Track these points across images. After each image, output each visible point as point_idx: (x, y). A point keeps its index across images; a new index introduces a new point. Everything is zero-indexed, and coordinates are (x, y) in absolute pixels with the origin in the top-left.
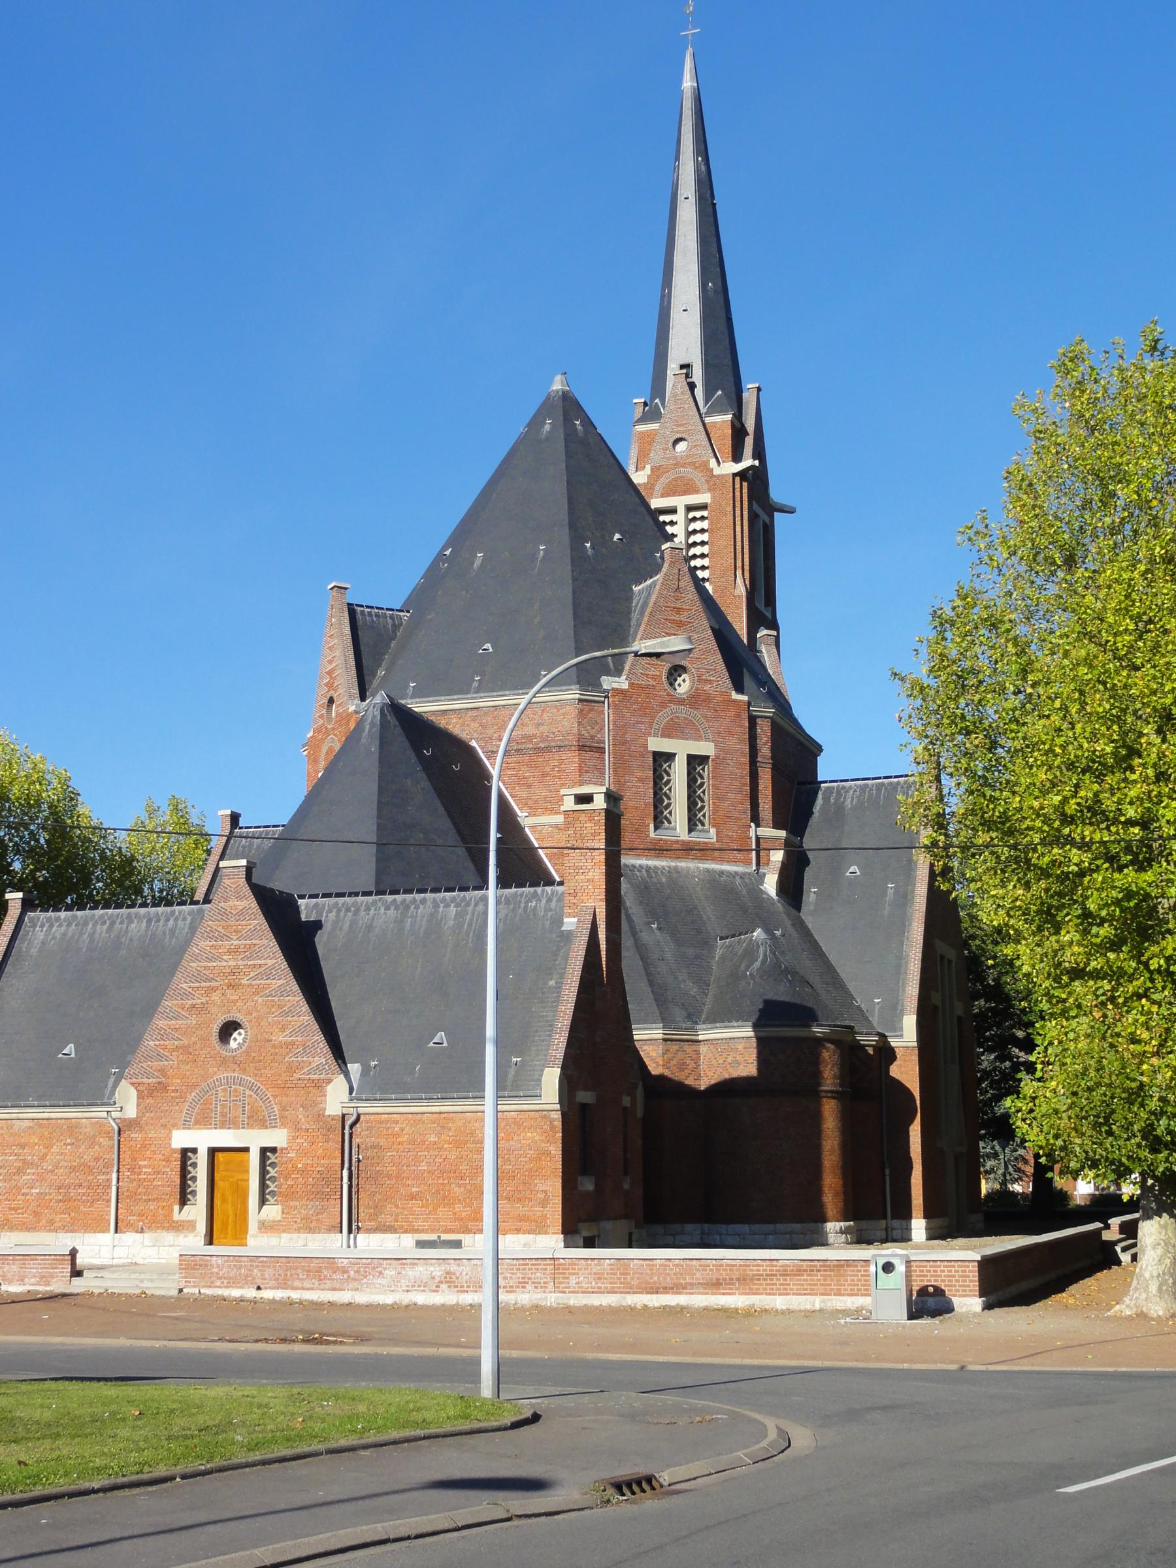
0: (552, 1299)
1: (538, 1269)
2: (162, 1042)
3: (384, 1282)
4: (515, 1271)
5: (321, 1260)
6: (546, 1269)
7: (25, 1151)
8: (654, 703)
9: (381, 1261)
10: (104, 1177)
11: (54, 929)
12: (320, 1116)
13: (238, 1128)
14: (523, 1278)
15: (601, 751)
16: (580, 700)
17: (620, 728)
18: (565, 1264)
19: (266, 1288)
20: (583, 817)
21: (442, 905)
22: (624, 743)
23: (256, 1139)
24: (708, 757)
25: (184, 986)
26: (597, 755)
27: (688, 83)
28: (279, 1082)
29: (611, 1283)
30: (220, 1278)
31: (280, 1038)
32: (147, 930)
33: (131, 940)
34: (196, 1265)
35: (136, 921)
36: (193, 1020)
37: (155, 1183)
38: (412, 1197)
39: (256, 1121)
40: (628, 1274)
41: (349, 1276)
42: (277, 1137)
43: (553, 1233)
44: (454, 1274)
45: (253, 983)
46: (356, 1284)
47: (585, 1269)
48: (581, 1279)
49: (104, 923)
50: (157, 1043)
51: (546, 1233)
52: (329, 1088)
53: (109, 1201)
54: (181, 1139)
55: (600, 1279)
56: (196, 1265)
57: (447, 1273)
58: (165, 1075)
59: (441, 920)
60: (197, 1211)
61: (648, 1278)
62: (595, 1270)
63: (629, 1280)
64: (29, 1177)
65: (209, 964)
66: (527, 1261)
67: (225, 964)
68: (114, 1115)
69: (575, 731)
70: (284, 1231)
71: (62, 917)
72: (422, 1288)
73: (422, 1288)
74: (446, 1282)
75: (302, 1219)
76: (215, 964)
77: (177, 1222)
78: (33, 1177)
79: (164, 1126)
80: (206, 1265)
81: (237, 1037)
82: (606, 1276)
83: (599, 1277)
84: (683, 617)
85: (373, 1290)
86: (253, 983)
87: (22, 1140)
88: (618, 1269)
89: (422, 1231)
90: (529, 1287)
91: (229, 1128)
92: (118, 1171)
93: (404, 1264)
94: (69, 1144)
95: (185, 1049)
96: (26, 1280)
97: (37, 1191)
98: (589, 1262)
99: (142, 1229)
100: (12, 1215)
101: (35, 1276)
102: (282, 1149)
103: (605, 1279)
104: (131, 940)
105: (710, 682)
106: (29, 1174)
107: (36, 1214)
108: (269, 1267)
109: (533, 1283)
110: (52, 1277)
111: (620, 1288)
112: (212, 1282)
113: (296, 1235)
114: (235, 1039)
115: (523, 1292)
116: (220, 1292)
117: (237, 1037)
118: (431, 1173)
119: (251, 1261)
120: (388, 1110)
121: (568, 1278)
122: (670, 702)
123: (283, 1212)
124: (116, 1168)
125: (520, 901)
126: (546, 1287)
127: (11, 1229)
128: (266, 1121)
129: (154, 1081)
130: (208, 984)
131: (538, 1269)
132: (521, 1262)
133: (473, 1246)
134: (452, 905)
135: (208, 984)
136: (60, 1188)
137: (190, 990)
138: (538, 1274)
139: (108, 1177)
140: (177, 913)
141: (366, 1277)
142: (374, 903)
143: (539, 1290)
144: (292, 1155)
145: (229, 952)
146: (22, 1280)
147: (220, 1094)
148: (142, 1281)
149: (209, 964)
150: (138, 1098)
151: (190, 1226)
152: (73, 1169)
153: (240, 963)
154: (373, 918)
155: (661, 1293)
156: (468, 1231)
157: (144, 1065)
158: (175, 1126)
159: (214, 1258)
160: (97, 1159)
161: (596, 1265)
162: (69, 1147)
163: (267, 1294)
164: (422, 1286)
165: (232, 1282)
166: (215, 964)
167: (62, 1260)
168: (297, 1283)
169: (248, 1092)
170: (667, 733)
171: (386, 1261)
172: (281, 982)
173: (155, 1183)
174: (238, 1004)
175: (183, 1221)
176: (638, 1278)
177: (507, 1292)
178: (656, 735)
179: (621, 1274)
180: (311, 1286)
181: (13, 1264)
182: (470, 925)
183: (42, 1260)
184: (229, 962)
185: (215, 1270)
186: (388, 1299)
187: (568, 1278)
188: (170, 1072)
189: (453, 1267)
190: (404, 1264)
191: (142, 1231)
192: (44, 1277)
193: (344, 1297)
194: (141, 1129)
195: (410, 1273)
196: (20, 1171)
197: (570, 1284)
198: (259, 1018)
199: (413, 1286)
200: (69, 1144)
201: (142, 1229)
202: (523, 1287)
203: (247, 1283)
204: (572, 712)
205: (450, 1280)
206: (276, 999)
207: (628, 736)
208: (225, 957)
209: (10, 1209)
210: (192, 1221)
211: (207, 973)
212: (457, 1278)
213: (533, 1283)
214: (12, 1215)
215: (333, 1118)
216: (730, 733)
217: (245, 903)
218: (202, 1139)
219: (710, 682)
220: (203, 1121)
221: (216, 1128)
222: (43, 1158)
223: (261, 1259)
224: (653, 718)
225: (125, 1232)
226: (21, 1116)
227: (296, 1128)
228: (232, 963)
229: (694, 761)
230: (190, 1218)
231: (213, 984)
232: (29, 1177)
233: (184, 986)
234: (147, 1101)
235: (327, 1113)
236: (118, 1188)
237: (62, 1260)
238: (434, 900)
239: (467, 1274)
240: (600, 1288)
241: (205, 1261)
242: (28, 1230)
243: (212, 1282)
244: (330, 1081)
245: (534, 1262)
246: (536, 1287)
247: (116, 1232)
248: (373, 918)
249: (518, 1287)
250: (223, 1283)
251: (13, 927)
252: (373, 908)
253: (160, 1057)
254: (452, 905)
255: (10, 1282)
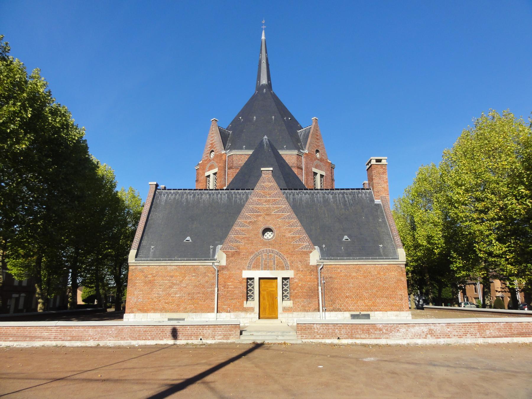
0: (480, 341)
1: (471, 327)
2: (237, 236)
3: (400, 334)
4: (461, 328)
5: (368, 325)
6: (475, 327)
7: (173, 279)
8: (313, 159)
9: (398, 325)
10: (210, 289)
11: (170, 196)
12: (307, 265)
13: (272, 270)
14: (465, 331)
15: (302, 169)
16: (297, 154)
17: (307, 164)
18: (483, 325)
19: (342, 338)
20: (379, 166)
21: (326, 194)
22: (308, 168)
23: (280, 274)
24: (323, 176)
25: (246, 214)
26: (301, 170)
27: (263, 37)
28: (289, 252)
29: (505, 333)
30: (319, 334)
31: (289, 235)
32: (210, 198)
33: (204, 201)
34: (306, 328)
35: (204, 195)
36: (251, 227)
37: (235, 292)
38: (347, 297)
39: (280, 267)
40: (512, 329)
41: (383, 332)
42: (289, 274)
43: (406, 311)
44: (433, 330)
45: (277, 214)
46: (387, 336)
47: (493, 327)
48: (492, 331)
49: (191, 195)
50: (235, 236)
51: (403, 311)
52: (311, 254)
53: (214, 299)
54: (246, 274)
55: (500, 331)
56: (306, 328)
57: (430, 330)
58: (239, 249)
59: (328, 199)
60: (254, 304)
61: (520, 330)
62: (497, 327)
63: (513, 332)
64: (175, 290)
65: (257, 206)
66: (466, 324)
67: (264, 206)
68: (217, 264)
69: (296, 163)
70: (294, 311)
71: (172, 192)
72: (419, 337)
73: (419, 337)
74: (430, 334)
75: (302, 306)
76: (260, 206)
77: (246, 308)
78: (177, 290)
79: (239, 269)
80: (311, 328)
81: (267, 235)
82: (502, 330)
83: (499, 330)
84: (318, 137)
85: (396, 338)
86: (277, 214)
87: (171, 274)
88: (507, 327)
89: (352, 311)
90: (468, 335)
91: (268, 270)
92: (218, 287)
93: (409, 326)
94: (194, 276)
95: (248, 239)
96: (216, 337)
97: (179, 295)
98: (494, 324)
99: (230, 311)
100: (166, 306)
101: (221, 335)
102: (292, 278)
103: (502, 331)
104: (204, 201)
105: (324, 156)
106: (174, 288)
107: (178, 305)
108: (343, 328)
109: (470, 333)
110: (230, 335)
111: (509, 335)
112: (315, 336)
113: (300, 313)
114: (266, 236)
115: (466, 338)
116: (320, 341)
117: (267, 235)
118: (354, 288)
119: (334, 326)
120: (336, 263)
121: (485, 331)
122: (316, 159)
123: (293, 304)
124: (217, 286)
125: (355, 194)
126: (476, 335)
127: (166, 312)
128: (284, 267)
129: (234, 251)
130: (257, 214)
131: (471, 327)
132: (463, 324)
133: (375, 316)
134: (330, 194)
135: (257, 214)
136: (189, 294)
137: (249, 216)
138: (472, 330)
139: (212, 289)
140: (221, 193)
141: (391, 332)
142: (299, 192)
143: (473, 337)
144: (296, 280)
145: (266, 202)
146: (214, 337)
147: (264, 257)
148: (278, 336)
149: (257, 206)
150: (227, 257)
151: (252, 309)
152: (196, 286)
153: (271, 206)
154: (301, 197)
155: (528, 337)
156: (372, 311)
157: (229, 244)
158: (244, 269)
159: (315, 325)
160: (207, 282)
161: (497, 325)
162: (193, 277)
163: (344, 341)
164: (419, 336)
165: (325, 336)
166: (260, 206)
167: (235, 327)
168: (358, 336)
169: (276, 256)
170: (317, 167)
171: (401, 325)
172: (289, 214)
173: (235, 292)
174: (270, 222)
175: (247, 308)
176: (517, 331)
177: (459, 338)
178: (314, 167)
179: (509, 329)
180: (365, 337)
181: (209, 329)
182: (339, 201)
183: (224, 327)
184: (266, 206)
185: (316, 330)
186: (404, 342)
187: (485, 331)
188: (241, 247)
189: (432, 327)
190: (409, 326)
191: (230, 312)
192: (226, 335)
193: (383, 341)
194: (228, 270)
195: (412, 330)
196: (171, 287)
197: (487, 334)
198: (280, 227)
199: (414, 336)
200: (194, 276)
201: (230, 311)
202: (466, 335)
203: (332, 336)
204: (295, 157)
205: (431, 333)
206: (286, 220)
207: (308, 166)
208: (264, 204)
209: (166, 303)
210: (252, 308)
211: (256, 209)
212: (435, 332)
213: (470, 333)
214: (166, 306)
215: (313, 266)
216: (328, 170)
217: (272, 184)
218: (256, 274)
219: (324, 156)
220: (256, 267)
221: (262, 270)
222: (181, 282)
223: (339, 325)
224: (313, 162)
225: (222, 312)
226: (172, 264)
227: (297, 270)
228: (267, 206)
229: (322, 176)
230: (251, 306)
231: (259, 214)
232: (175, 290)
233: (246, 214)
234: (231, 259)
235: (310, 264)
236: (218, 294)
237: (235, 327)
238: (322, 193)
239: (439, 330)
240: (501, 335)
241: (312, 326)
242: (174, 312)
243: (315, 336)
244: (311, 252)
245: (469, 324)
246: (472, 335)
247: (217, 312)
248: (301, 197)
249: (463, 335)
250: (320, 336)
251: (153, 194)
252: (300, 194)
253: (237, 242)
254: (330, 194)
255: (207, 338)
